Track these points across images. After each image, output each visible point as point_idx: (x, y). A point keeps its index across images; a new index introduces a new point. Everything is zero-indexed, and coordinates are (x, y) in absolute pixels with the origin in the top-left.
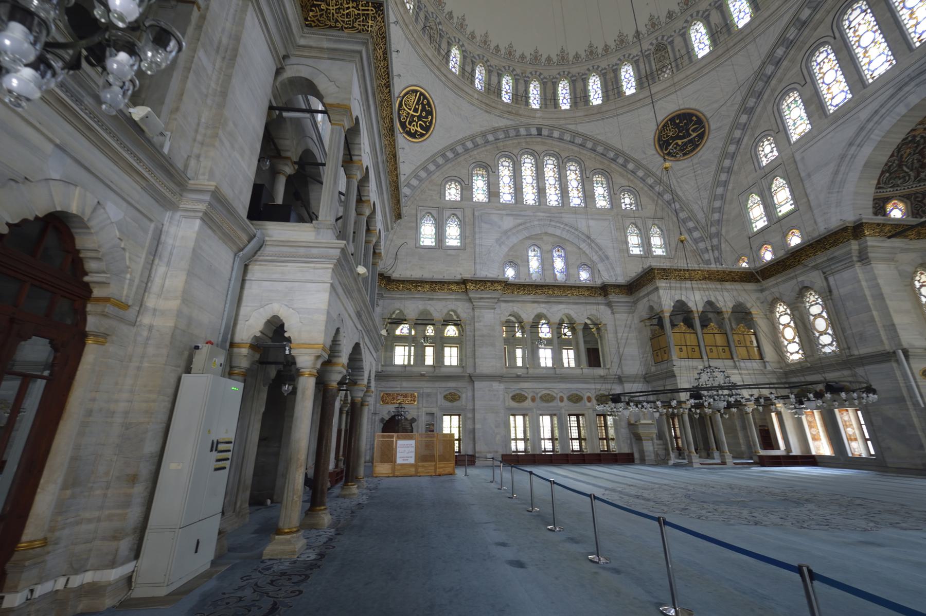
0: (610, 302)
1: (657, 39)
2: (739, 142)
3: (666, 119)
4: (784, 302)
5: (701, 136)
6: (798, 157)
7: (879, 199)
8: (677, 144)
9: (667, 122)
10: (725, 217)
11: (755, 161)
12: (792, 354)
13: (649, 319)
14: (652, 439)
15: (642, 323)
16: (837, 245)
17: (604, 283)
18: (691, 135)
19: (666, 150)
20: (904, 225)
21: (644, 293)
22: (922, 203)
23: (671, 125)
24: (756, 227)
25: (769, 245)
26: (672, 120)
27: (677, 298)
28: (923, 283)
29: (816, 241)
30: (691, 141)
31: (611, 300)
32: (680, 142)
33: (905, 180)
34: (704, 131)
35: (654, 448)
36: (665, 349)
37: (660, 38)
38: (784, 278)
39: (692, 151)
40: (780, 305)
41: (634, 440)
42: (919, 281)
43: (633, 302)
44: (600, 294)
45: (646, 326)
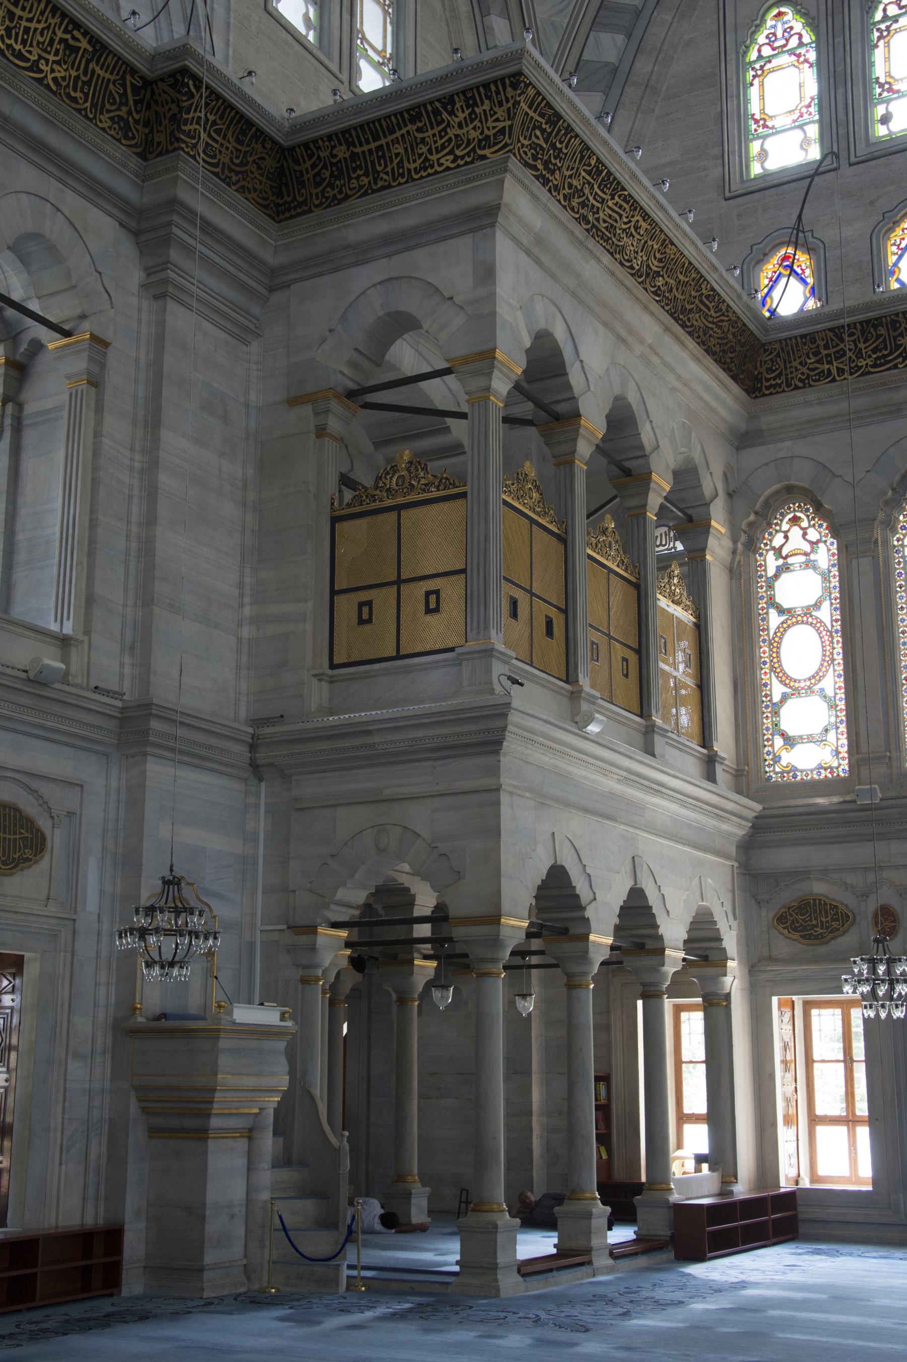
0: (173, 205)
4: (819, 509)
10: (644, 66)
12: (790, 741)
13: (351, 395)
14: (250, 1134)
15: (306, 410)
17: (184, 50)
21: (383, 227)
24: (763, 155)
25: (809, 250)
27: (542, 324)
31: (185, 196)
35: (250, 1190)
36: (432, 585)
38: (861, 402)
40: (795, 520)
41: (137, 1135)
43: (274, 272)
44: (124, 130)
45: (321, 432)
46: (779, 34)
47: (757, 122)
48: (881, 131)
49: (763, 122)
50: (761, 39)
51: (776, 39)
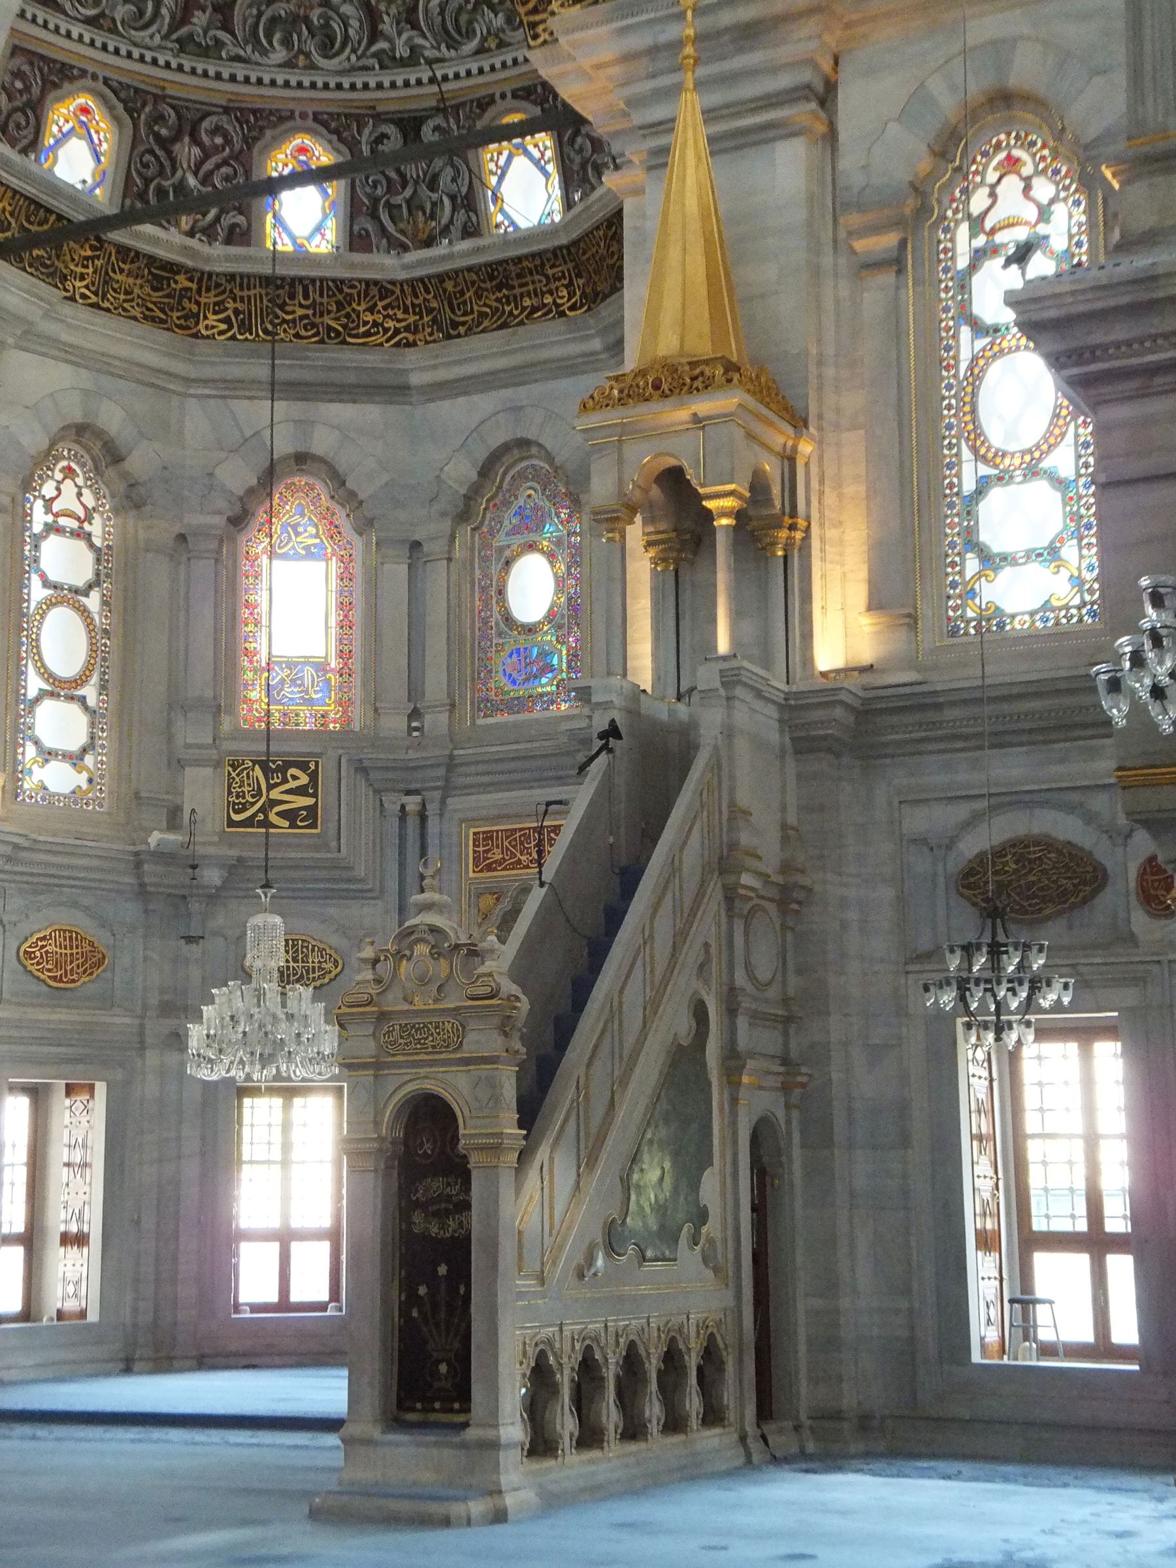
7: (32, 56)
20: (60, 217)
22: (169, 153)
28: (56, 515)
33: (141, 13)
42: (48, 503)
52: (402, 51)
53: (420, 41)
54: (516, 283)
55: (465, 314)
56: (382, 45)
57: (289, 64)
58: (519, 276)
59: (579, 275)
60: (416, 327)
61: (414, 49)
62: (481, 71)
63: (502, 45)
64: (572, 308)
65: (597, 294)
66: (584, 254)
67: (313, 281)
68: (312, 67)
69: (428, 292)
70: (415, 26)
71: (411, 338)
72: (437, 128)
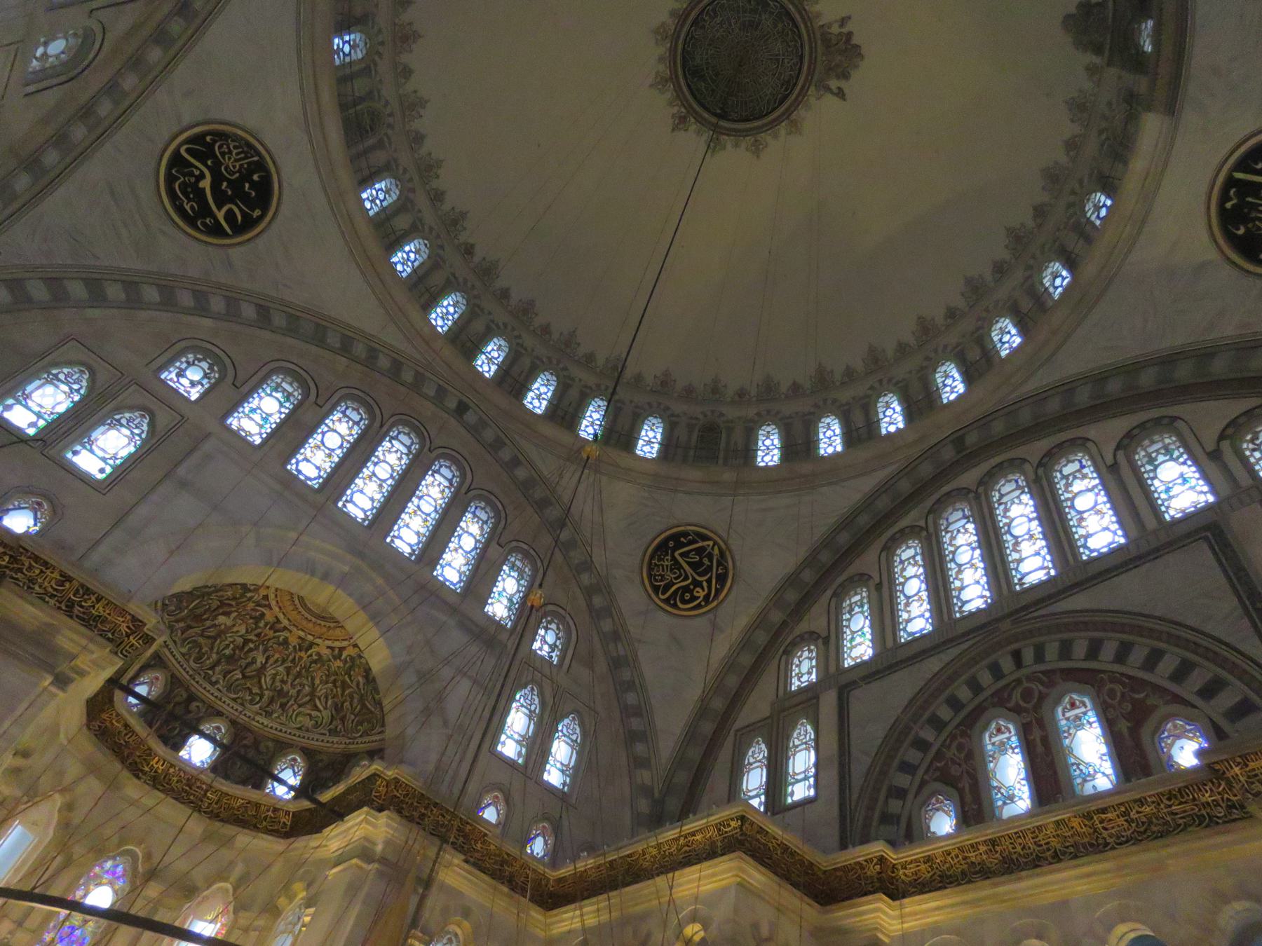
1: (391, 115)
2: (201, 308)
3: (263, 152)
5: (216, 231)
6: (208, 446)
8: (202, 176)
9: (258, 153)
11: (167, 355)
16: (88, 626)
18: (219, 208)
19: (188, 150)
23: (248, 164)
26: (261, 166)
29: (82, 586)
30: (205, 211)
32: (206, 184)
34: (225, 235)
37: (391, 120)
39: (180, 210)
46: (74, 377)
47: (24, 393)
48: (69, 455)
49: (27, 397)
50: (66, 371)
51: (71, 378)
52: (214, 679)
53: (221, 681)
54: (194, 788)
55: (167, 784)
56: (210, 672)
57: (183, 655)
58: (198, 787)
59: (216, 803)
60: (146, 773)
61: (217, 682)
62: (228, 705)
63: (242, 704)
64: (204, 812)
65: (217, 816)
66: (228, 800)
67: (137, 735)
68: (187, 661)
69: (162, 765)
70: (224, 677)
71: (140, 774)
72: (198, 707)
